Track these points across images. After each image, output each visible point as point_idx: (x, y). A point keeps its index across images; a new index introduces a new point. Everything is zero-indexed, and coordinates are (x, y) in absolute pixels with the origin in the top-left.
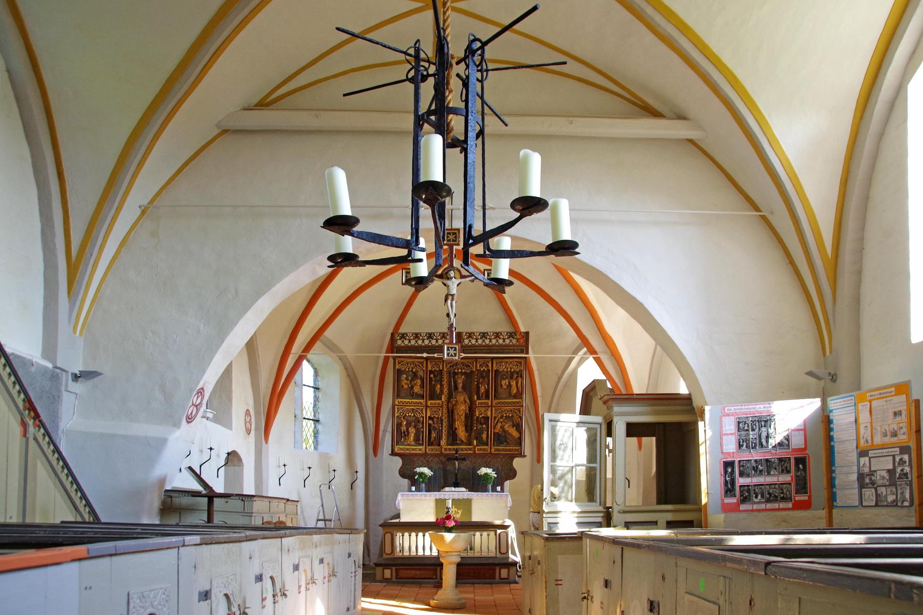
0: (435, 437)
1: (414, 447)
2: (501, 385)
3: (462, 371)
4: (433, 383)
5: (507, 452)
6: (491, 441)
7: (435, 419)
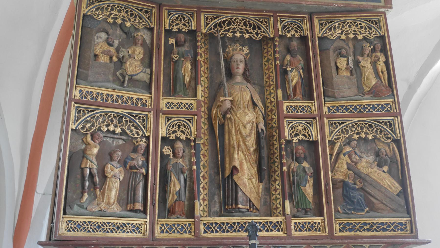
0: (179, 193)
1: (120, 221)
2: (337, 67)
3: (242, 37)
4: (175, 57)
5: (375, 233)
6: (328, 203)
7: (179, 145)
